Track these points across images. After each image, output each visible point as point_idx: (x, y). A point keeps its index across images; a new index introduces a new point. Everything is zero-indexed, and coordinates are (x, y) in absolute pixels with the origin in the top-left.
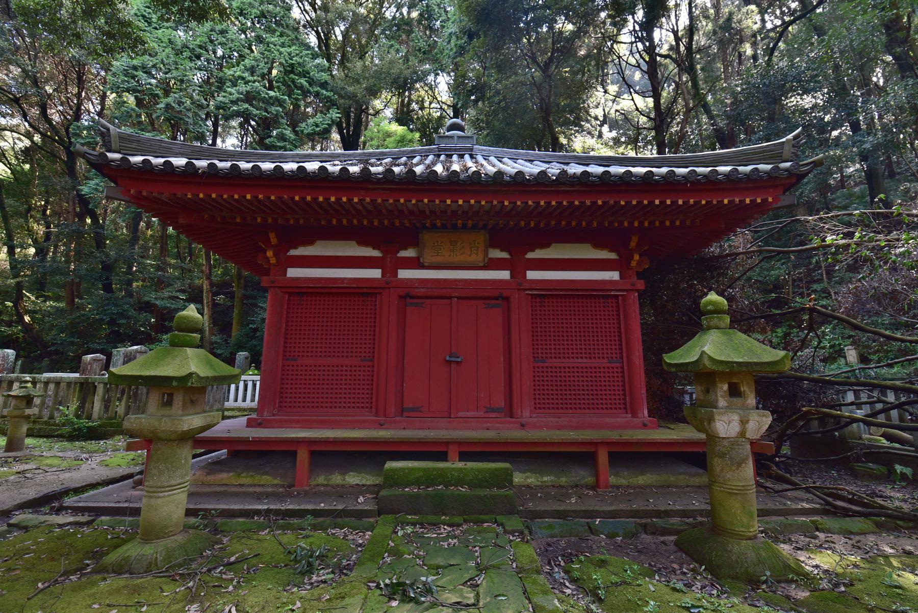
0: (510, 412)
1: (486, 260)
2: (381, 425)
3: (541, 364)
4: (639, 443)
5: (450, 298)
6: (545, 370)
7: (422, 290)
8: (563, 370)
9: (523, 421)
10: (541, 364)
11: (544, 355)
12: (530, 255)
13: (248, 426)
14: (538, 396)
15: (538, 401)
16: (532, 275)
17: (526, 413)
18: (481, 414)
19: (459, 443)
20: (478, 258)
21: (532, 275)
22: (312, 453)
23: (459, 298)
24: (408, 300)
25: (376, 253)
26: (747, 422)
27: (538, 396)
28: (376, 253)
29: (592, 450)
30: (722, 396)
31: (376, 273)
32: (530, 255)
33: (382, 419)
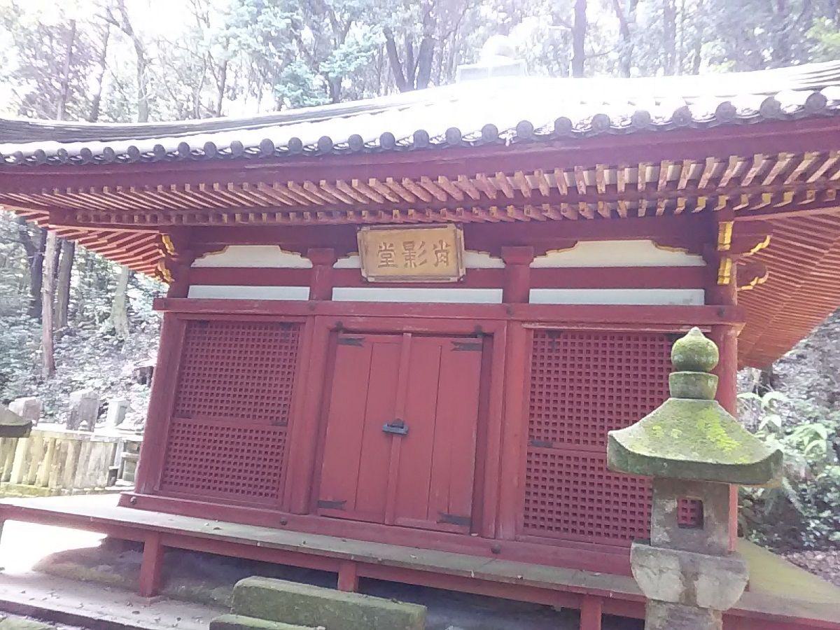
0: (474, 523)
1: (462, 272)
2: (284, 523)
3: (546, 451)
4: (519, 586)
5: (401, 333)
6: (549, 460)
7: (360, 320)
8: (581, 463)
9: (496, 544)
10: (546, 451)
11: (550, 435)
12: (539, 262)
13: (121, 504)
14: (532, 506)
15: (532, 514)
16: (539, 296)
17: (507, 531)
18: (432, 523)
19: (358, 563)
20: (448, 268)
21: (539, 296)
22: (163, 549)
23: (414, 334)
24: (342, 335)
25: (305, 263)
26: (696, 575)
27: (532, 506)
28: (305, 263)
29: (572, 605)
30: (659, 523)
31: (300, 293)
32: (539, 262)
33: (284, 515)
